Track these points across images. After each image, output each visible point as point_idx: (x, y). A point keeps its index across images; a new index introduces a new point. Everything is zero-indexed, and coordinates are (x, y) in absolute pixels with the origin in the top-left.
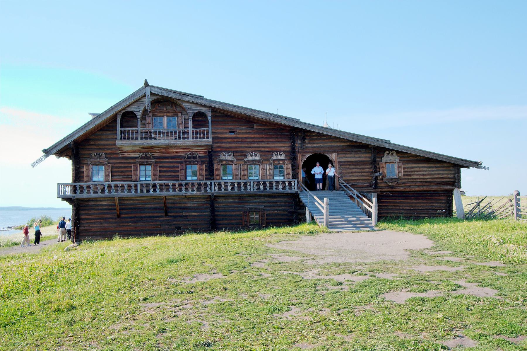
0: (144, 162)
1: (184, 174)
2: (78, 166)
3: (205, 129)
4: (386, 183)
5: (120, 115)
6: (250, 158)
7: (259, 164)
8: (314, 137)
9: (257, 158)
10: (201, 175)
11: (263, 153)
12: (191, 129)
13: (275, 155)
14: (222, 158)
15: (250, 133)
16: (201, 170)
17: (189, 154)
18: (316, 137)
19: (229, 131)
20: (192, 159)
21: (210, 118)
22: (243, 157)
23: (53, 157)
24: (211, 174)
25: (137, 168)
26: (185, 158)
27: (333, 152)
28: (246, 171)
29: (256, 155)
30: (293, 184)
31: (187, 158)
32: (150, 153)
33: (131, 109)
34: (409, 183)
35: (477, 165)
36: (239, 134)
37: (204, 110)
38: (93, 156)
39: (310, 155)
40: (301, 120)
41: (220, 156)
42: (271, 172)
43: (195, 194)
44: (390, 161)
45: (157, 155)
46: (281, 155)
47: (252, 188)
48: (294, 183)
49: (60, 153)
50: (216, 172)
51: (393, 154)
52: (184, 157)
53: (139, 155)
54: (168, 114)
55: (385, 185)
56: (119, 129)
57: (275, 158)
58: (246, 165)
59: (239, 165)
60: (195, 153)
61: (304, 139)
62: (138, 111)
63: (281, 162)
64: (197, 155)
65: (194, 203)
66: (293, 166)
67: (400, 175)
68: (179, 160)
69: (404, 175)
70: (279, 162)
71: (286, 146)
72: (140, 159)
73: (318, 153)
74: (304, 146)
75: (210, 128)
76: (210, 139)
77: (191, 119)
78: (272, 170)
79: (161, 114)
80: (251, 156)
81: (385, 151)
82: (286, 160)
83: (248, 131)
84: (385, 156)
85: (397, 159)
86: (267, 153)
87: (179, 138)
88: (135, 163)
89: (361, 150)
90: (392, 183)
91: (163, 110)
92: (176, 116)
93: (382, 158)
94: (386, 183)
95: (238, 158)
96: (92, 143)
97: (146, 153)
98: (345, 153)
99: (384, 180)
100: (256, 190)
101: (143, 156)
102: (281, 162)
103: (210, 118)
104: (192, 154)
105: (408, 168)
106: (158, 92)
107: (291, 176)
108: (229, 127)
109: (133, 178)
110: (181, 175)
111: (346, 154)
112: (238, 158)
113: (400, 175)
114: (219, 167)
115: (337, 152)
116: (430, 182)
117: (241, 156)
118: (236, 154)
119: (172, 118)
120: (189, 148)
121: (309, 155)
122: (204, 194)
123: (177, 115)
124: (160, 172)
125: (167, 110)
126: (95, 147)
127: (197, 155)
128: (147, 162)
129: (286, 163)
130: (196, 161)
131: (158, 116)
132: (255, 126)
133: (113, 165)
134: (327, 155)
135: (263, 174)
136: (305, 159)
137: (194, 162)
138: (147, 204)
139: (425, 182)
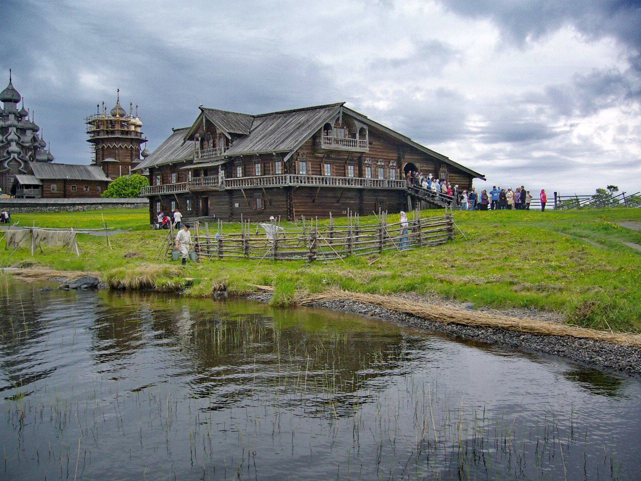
6: (379, 163)
9: (383, 164)
14: (366, 162)
16: (356, 170)
22: (376, 163)
24: (361, 173)
35: (482, 177)
37: (365, 127)
47: (386, 186)
57: (391, 164)
71: (394, 155)
105: (452, 176)
121: (406, 164)
123: (343, 128)
124: (336, 169)
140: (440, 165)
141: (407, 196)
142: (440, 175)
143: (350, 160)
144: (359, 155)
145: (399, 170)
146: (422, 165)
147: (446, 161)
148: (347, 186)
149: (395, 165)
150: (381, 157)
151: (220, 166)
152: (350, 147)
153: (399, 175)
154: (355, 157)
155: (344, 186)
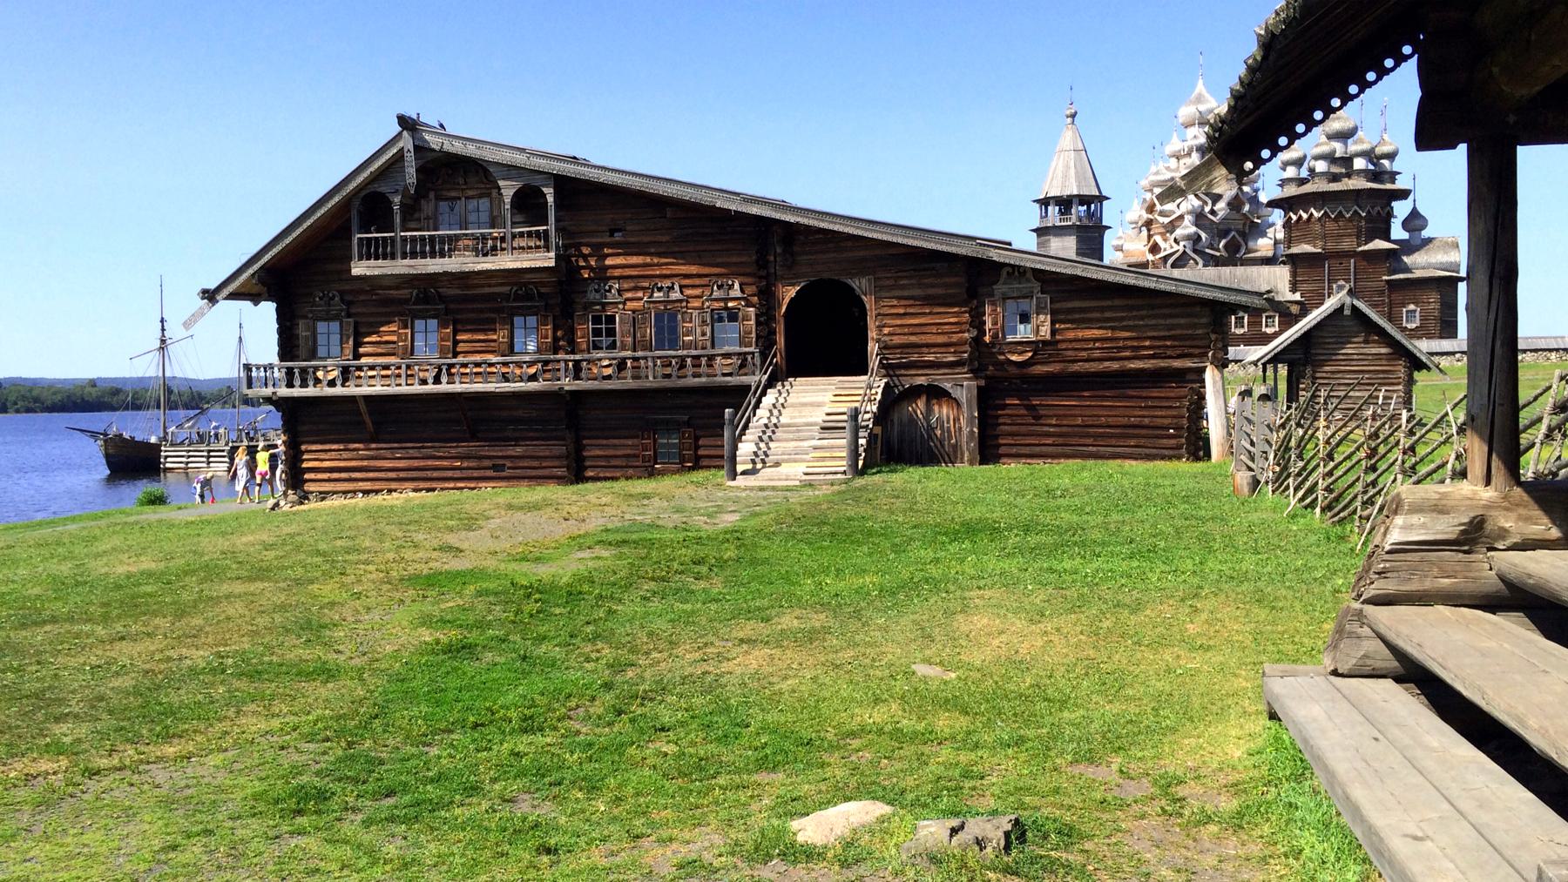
2: (288, 324)
5: (357, 203)
21: (550, 199)
22: (640, 294)
23: (226, 307)
26: (508, 301)
37: (536, 181)
39: (802, 284)
41: (586, 292)
49: (233, 296)
52: (506, 297)
54: (470, 193)
69: (1053, 332)
70: (726, 304)
72: (414, 304)
73: (826, 276)
76: (552, 254)
78: (707, 325)
79: (453, 194)
81: (1001, 269)
84: (1002, 280)
85: (1037, 286)
86: (697, 281)
90: (1021, 353)
91: (458, 184)
93: (994, 287)
95: (629, 295)
103: (550, 199)
112: (629, 295)
116: (1134, 348)
117: (636, 289)
125: (466, 183)
128: (427, 310)
130: (536, 307)
133: (359, 319)
134: (849, 281)
137: (530, 307)
139: (1120, 349)
143: (517, 298)
147: (995, 255)
154: (543, 284)
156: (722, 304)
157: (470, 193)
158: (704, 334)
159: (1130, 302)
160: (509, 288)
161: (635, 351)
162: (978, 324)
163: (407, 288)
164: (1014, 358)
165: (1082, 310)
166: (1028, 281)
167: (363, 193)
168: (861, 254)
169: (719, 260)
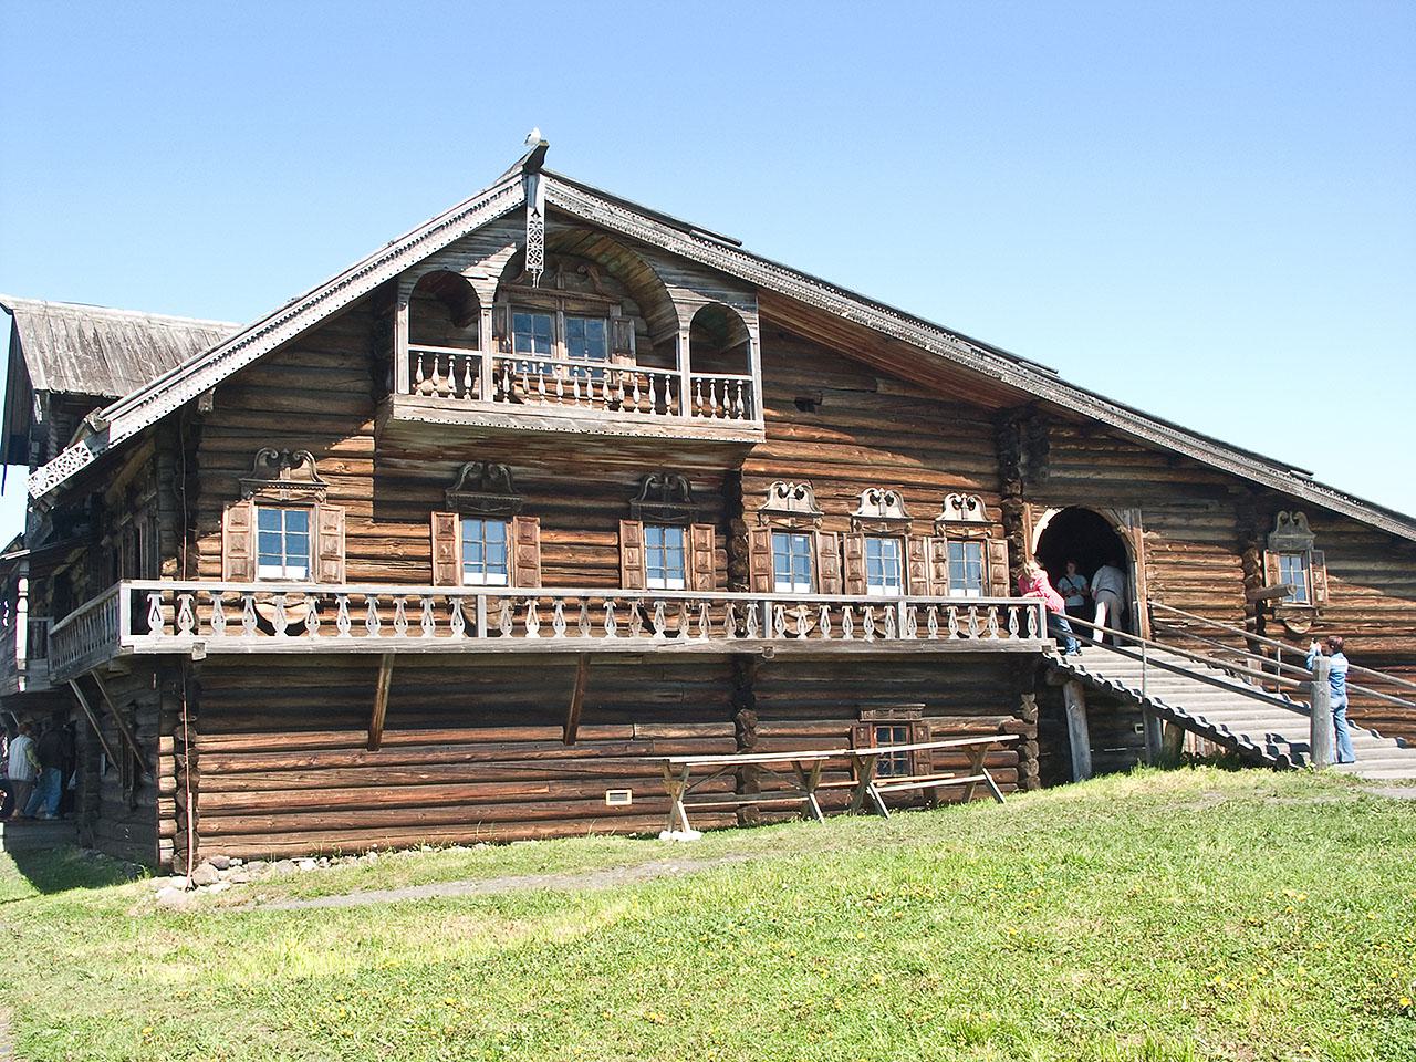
0: (478, 503)
1: (640, 562)
3: (740, 378)
4: (1283, 623)
5: (409, 286)
6: (868, 510)
7: (902, 537)
8: (1068, 447)
9: (894, 512)
10: (702, 570)
11: (911, 494)
12: (685, 373)
13: (954, 503)
14: (774, 503)
15: (864, 413)
16: (702, 548)
17: (652, 481)
18: (1073, 446)
19: (792, 398)
20: (667, 502)
22: (845, 506)
25: (451, 527)
27: (1129, 502)
28: (859, 561)
29: (889, 501)
30: (1032, 616)
31: (649, 498)
32: (502, 467)
33: (449, 263)
34: (1342, 626)
36: (830, 410)
37: (734, 302)
38: (263, 463)
40: (1062, 376)
41: (767, 494)
42: (944, 568)
43: (704, 649)
44: (1290, 548)
45: (528, 477)
46: (972, 506)
48: (1037, 614)
50: (756, 562)
51: (1296, 521)
53: (458, 470)
54: (574, 307)
55: (1280, 629)
56: (403, 347)
57: (951, 514)
58: (859, 536)
59: (836, 534)
60: (679, 477)
61: (1038, 451)
62: (485, 276)
63: (972, 533)
64: (685, 486)
65: (678, 689)
66: (1012, 548)
67: (1320, 598)
68: (613, 505)
70: (966, 531)
72: (462, 489)
74: (1044, 474)
75: (756, 377)
76: (759, 422)
77: (684, 329)
78: (944, 561)
80: (874, 500)
82: (989, 525)
83: (859, 404)
85: (1310, 538)
87: (614, 406)
88: (442, 507)
89: (1207, 501)
92: (603, 317)
94: (1283, 623)
95: (828, 506)
96: (256, 403)
97: (486, 466)
98: (1164, 510)
99: (1277, 613)
100: (915, 638)
101: (471, 476)
102: (972, 533)
103: (754, 333)
104: (667, 480)
106: (570, 201)
107: (1007, 588)
108: (798, 380)
109: (437, 573)
110: (627, 569)
111: (1189, 517)
113: (1320, 598)
114: (774, 542)
115: (1139, 505)
116: (1396, 623)
118: (821, 492)
119: (587, 324)
120: (662, 456)
121: (1051, 513)
122: (738, 650)
126: (268, 423)
127: (685, 486)
128: (492, 503)
129: (989, 537)
131: (533, 311)
132: (881, 388)
134: (1108, 513)
135: (917, 576)
136: (1043, 524)
138: (490, 692)
140: (1273, 515)
141: (1060, 689)
142: (1273, 568)
143: (654, 496)
144: (713, 464)
145: (1002, 548)
146: (1154, 520)
148: (610, 640)
149: (975, 515)
150: (882, 476)
151: (25, 568)
152: (621, 414)
153: (1004, 571)
154: (695, 475)
155: (586, 641)
156: (961, 532)
157: (574, 307)
158: (938, 576)
159: (1392, 567)
160: (637, 475)
161: (844, 593)
162: (1252, 582)
163: (458, 460)
164: (1296, 628)
165: (1372, 573)
166: (1301, 531)
167: (422, 272)
168: (1122, 476)
169: (953, 466)
